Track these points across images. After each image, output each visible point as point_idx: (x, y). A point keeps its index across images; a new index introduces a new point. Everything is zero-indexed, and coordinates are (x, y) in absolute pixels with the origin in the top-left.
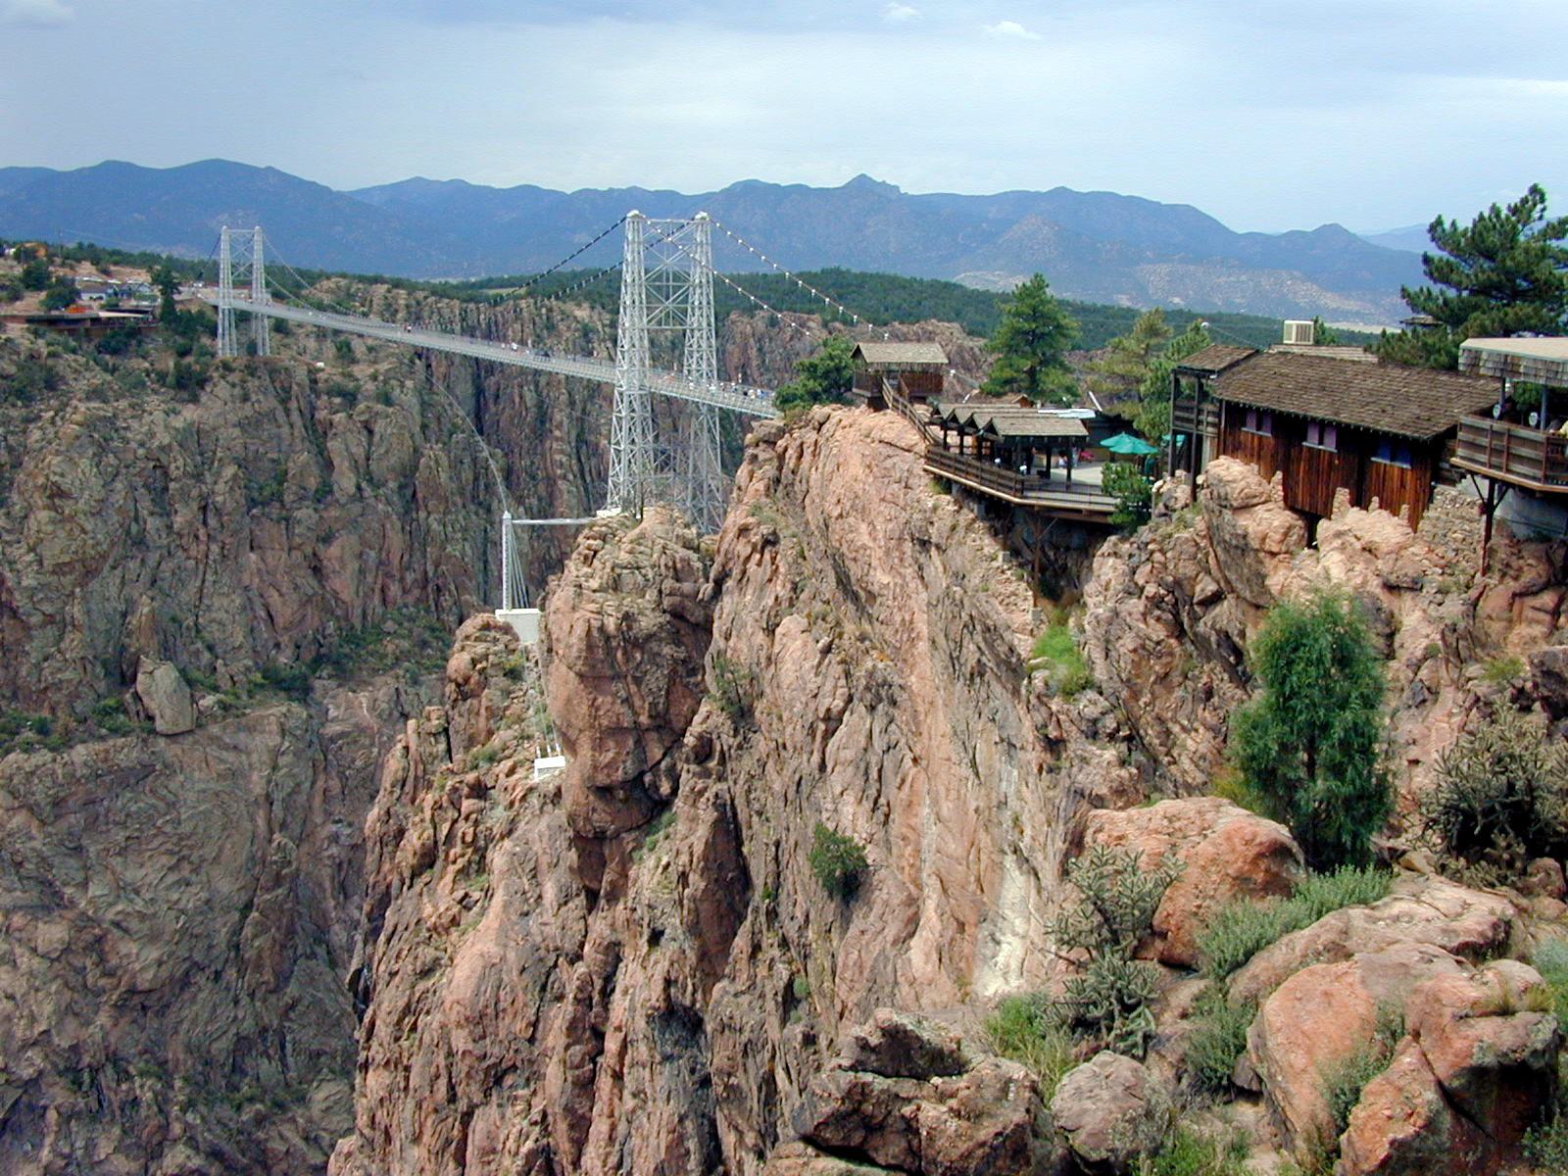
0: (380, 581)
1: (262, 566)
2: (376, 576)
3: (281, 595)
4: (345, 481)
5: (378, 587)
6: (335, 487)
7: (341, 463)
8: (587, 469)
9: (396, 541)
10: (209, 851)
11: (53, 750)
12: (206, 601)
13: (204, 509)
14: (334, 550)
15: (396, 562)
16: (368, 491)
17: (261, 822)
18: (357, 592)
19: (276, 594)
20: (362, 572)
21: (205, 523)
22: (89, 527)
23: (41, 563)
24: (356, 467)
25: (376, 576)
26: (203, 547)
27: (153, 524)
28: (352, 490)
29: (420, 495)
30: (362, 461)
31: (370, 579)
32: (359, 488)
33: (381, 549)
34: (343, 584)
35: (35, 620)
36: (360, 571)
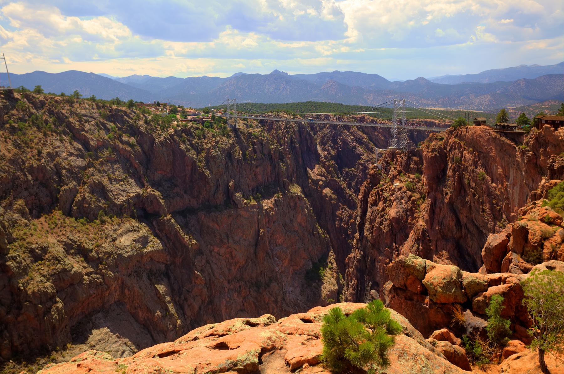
9: (269, 168)
11: (220, 212)
14: (258, 170)
20: (263, 174)
21: (238, 164)
24: (260, 152)
27: (230, 164)
28: (260, 157)
34: (260, 178)
35: (212, 185)
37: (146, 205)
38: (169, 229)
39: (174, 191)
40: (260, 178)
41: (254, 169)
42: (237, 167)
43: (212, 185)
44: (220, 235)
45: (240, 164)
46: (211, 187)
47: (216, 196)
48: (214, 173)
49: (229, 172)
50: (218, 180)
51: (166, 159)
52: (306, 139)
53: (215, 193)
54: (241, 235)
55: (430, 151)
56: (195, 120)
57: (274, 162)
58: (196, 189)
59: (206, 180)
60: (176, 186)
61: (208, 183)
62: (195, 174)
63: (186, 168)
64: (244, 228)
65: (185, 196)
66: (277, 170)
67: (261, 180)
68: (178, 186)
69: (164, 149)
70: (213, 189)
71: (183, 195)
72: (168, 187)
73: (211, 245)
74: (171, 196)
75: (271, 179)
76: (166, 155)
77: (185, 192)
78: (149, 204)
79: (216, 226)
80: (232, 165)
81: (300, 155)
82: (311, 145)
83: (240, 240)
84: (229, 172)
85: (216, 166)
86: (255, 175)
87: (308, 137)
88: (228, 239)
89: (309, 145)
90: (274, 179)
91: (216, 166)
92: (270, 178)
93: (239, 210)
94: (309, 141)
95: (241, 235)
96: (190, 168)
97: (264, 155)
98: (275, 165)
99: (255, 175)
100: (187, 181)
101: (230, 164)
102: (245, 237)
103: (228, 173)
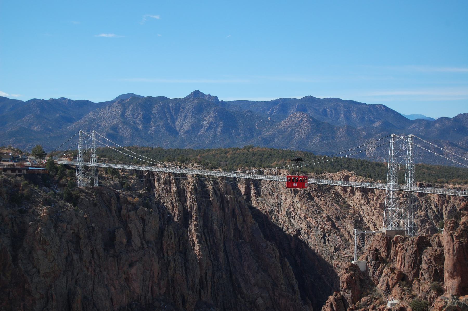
0: (151, 284)
2: (149, 282)
3: (115, 289)
4: (136, 241)
5: (150, 286)
6: (133, 243)
7: (134, 233)
8: (208, 238)
9: (156, 267)
13: (92, 251)
14: (133, 271)
15: (156, 276)
16: (145, 246)
18: (142, 289)
19: (113, 289)
21: (93, 257)
22: (56, 257)
23: (39, 272)
24: (139, 235)
25: (149, 282)
27: (76, 257)
28: (139, 245)
29: (164, 247)
31: (147, 283)
32: (142, 244)
33: (151, 271)
34: (137, 286)
35: (37, 296)
36: (143, 279)
40: (137, 286)
42: (90, 263)
43: (37, 296)
45: (96, 256)
48: (42, 273)
49: (73, 273)
50: (50, 286)
52: (234, 215)
56: (13, 169)
57: (166, 255)
59: (26, 286)
66: (171, 272)
67: (138, 291)
75: (160, 288)
80: (81, 259)
81: (222, 245)
82: (243, 227)
84: (73, 273)
87: (237, 211)
89: (240, 227)
90: (164, 289)
92: (156, 288)
94: (240, 219)
97: (148, 242)
98: (169, 262)
101: (76, 257)
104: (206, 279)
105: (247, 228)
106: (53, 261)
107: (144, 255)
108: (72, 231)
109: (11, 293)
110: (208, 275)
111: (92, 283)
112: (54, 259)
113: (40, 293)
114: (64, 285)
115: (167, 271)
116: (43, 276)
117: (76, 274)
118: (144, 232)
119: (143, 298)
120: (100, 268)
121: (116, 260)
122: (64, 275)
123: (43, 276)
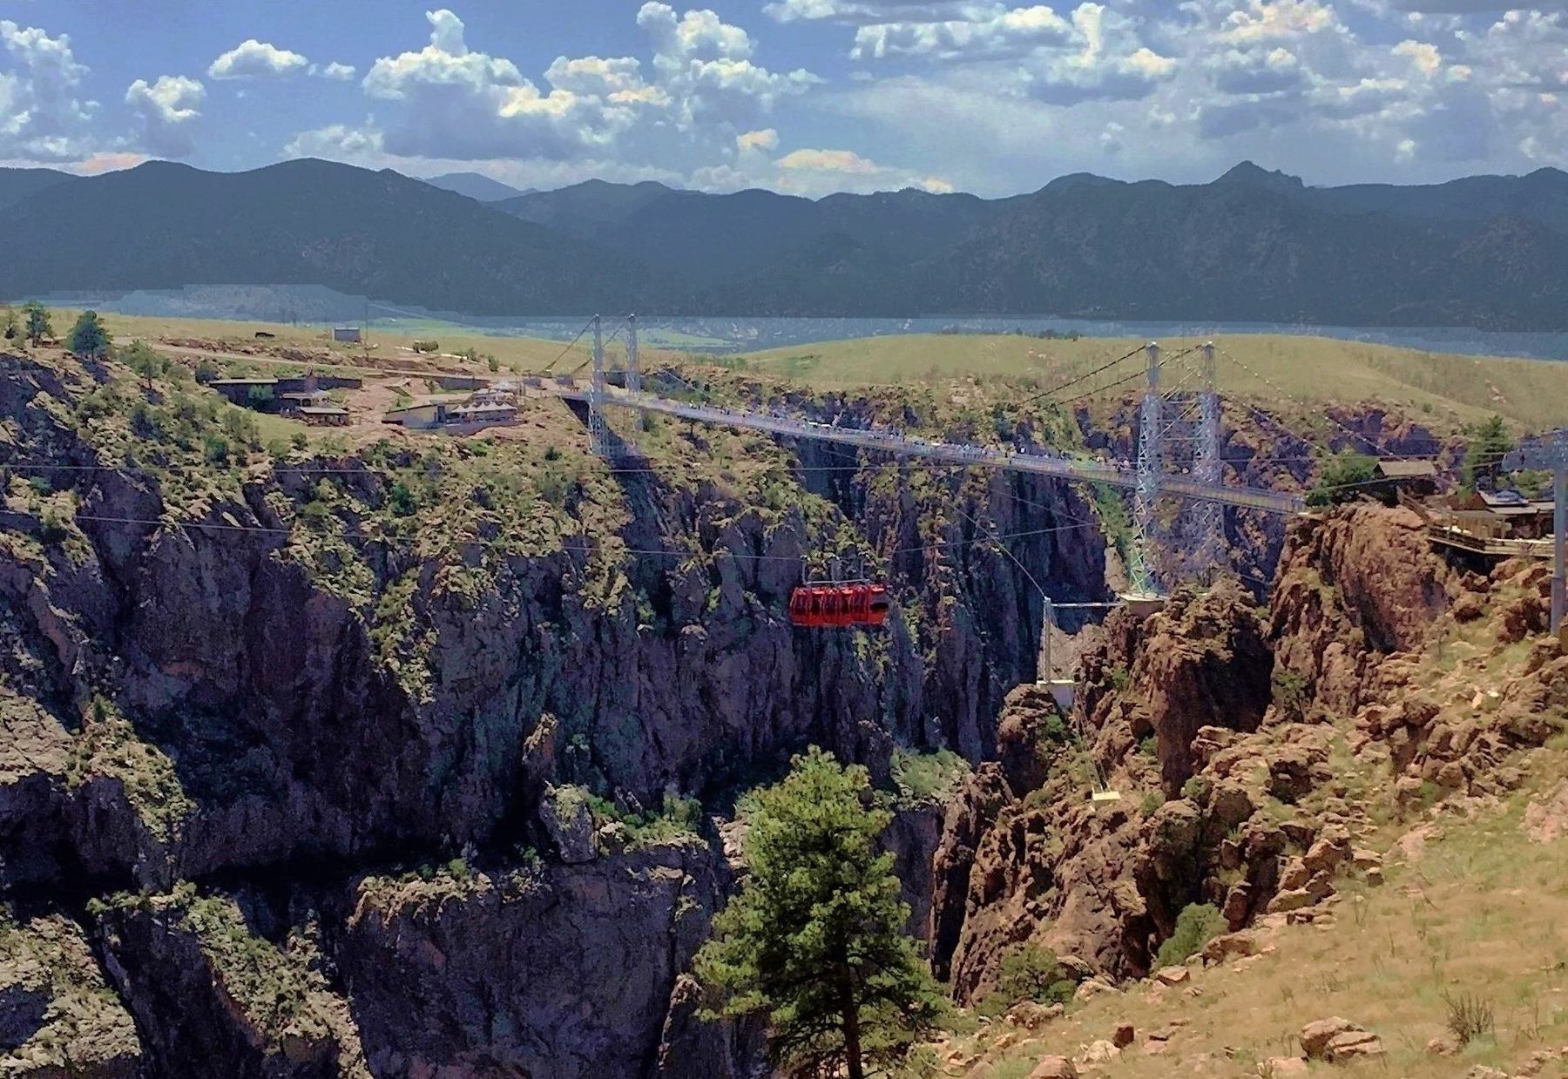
0: (770, 705)
1: (649, 686)
2: (767, 699)
5: (768, 713)
9: (788, 664)
10: (610, 991)
12: (601, 722)
15: (787, 683)
17: (662, 961)
18: (747, 717)
21: (598, 638)
25: (767, 699)
26: (597, 663)
30: (750, 574)
33: (772, 668)
34: (731, 709)
35: (434, 740)
37: (76, 833)
38: (166, 961)
39: (239, 764)
41: (698, 663)
42: (590, 654)
43: (434, 740)
44: (447, 997)
45: (606, 637)
46: (425, 749)
47: (446, 795)
49: (539, 681)
51: (215, 604)
53: (445, 780)
54: (568, 999)
55: (1183, 631)
58: (351, 757)
60: (256, 738)
61: (414, 731)
62: (351, 687)
63: (311, 652)
64: (588, 964)
65: (296, 791)
66: (826, 671)
67: (735, 721)
68: (267, 742)
69: (207, 555)
70: (436, 765)
71: (286, 787)
72: (210, 745)
73: (396, 1047)
74: (219, 788)
75: (797, 716)
76: (210, 585)
77: (300, 773)
78: (92, 825)
79: (429, 946)
81: (1011, 597)
82: (1071, 551)
83: (554, 1028)
84: (539, 681)
85: (461, 649)
86: (706, 694)
87: (1058, 507)
88: (489, 1019)
90: (809, 717)
91: (461, 649)
92: (786, 717)
93: (565, 871)
95: (568, 999)
96: (328, 653)
98: (822, 648)
99: (706, 694)
100: (312, 716)
102: (587, 1009)
103: (531, 681)
104: (964, 684)
105: (1085, 553)
106: (479, 649)
107: (753, 630)
108: (543, 574)
109: (367, 730)
110: (970, 674)
111: (593, 703)
112: (483, 646)
113: (442, 733)
114: (512, 712)
115: (818, 672)
116: (452, 690)
117: (547, 681)
118: (756, 569)
119: (749, 738)
120: (616, 666)
121: (672, 644)
122: (510, 685)
123: (452, 690)
